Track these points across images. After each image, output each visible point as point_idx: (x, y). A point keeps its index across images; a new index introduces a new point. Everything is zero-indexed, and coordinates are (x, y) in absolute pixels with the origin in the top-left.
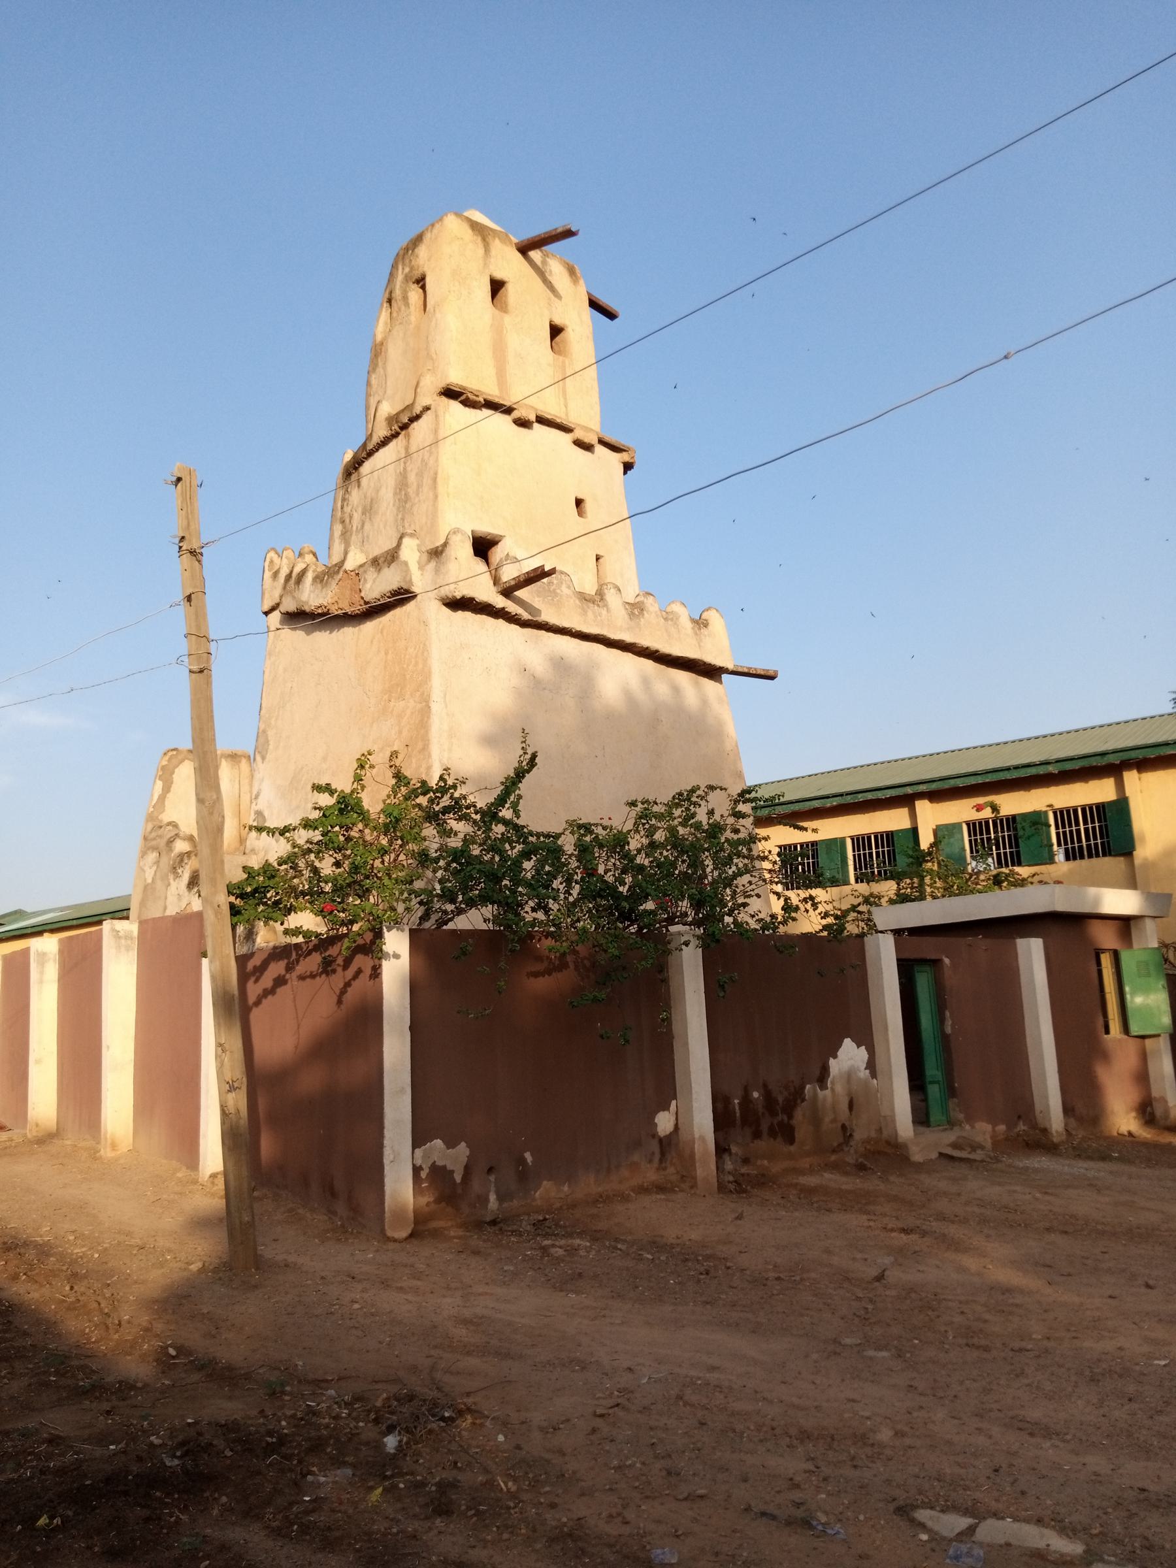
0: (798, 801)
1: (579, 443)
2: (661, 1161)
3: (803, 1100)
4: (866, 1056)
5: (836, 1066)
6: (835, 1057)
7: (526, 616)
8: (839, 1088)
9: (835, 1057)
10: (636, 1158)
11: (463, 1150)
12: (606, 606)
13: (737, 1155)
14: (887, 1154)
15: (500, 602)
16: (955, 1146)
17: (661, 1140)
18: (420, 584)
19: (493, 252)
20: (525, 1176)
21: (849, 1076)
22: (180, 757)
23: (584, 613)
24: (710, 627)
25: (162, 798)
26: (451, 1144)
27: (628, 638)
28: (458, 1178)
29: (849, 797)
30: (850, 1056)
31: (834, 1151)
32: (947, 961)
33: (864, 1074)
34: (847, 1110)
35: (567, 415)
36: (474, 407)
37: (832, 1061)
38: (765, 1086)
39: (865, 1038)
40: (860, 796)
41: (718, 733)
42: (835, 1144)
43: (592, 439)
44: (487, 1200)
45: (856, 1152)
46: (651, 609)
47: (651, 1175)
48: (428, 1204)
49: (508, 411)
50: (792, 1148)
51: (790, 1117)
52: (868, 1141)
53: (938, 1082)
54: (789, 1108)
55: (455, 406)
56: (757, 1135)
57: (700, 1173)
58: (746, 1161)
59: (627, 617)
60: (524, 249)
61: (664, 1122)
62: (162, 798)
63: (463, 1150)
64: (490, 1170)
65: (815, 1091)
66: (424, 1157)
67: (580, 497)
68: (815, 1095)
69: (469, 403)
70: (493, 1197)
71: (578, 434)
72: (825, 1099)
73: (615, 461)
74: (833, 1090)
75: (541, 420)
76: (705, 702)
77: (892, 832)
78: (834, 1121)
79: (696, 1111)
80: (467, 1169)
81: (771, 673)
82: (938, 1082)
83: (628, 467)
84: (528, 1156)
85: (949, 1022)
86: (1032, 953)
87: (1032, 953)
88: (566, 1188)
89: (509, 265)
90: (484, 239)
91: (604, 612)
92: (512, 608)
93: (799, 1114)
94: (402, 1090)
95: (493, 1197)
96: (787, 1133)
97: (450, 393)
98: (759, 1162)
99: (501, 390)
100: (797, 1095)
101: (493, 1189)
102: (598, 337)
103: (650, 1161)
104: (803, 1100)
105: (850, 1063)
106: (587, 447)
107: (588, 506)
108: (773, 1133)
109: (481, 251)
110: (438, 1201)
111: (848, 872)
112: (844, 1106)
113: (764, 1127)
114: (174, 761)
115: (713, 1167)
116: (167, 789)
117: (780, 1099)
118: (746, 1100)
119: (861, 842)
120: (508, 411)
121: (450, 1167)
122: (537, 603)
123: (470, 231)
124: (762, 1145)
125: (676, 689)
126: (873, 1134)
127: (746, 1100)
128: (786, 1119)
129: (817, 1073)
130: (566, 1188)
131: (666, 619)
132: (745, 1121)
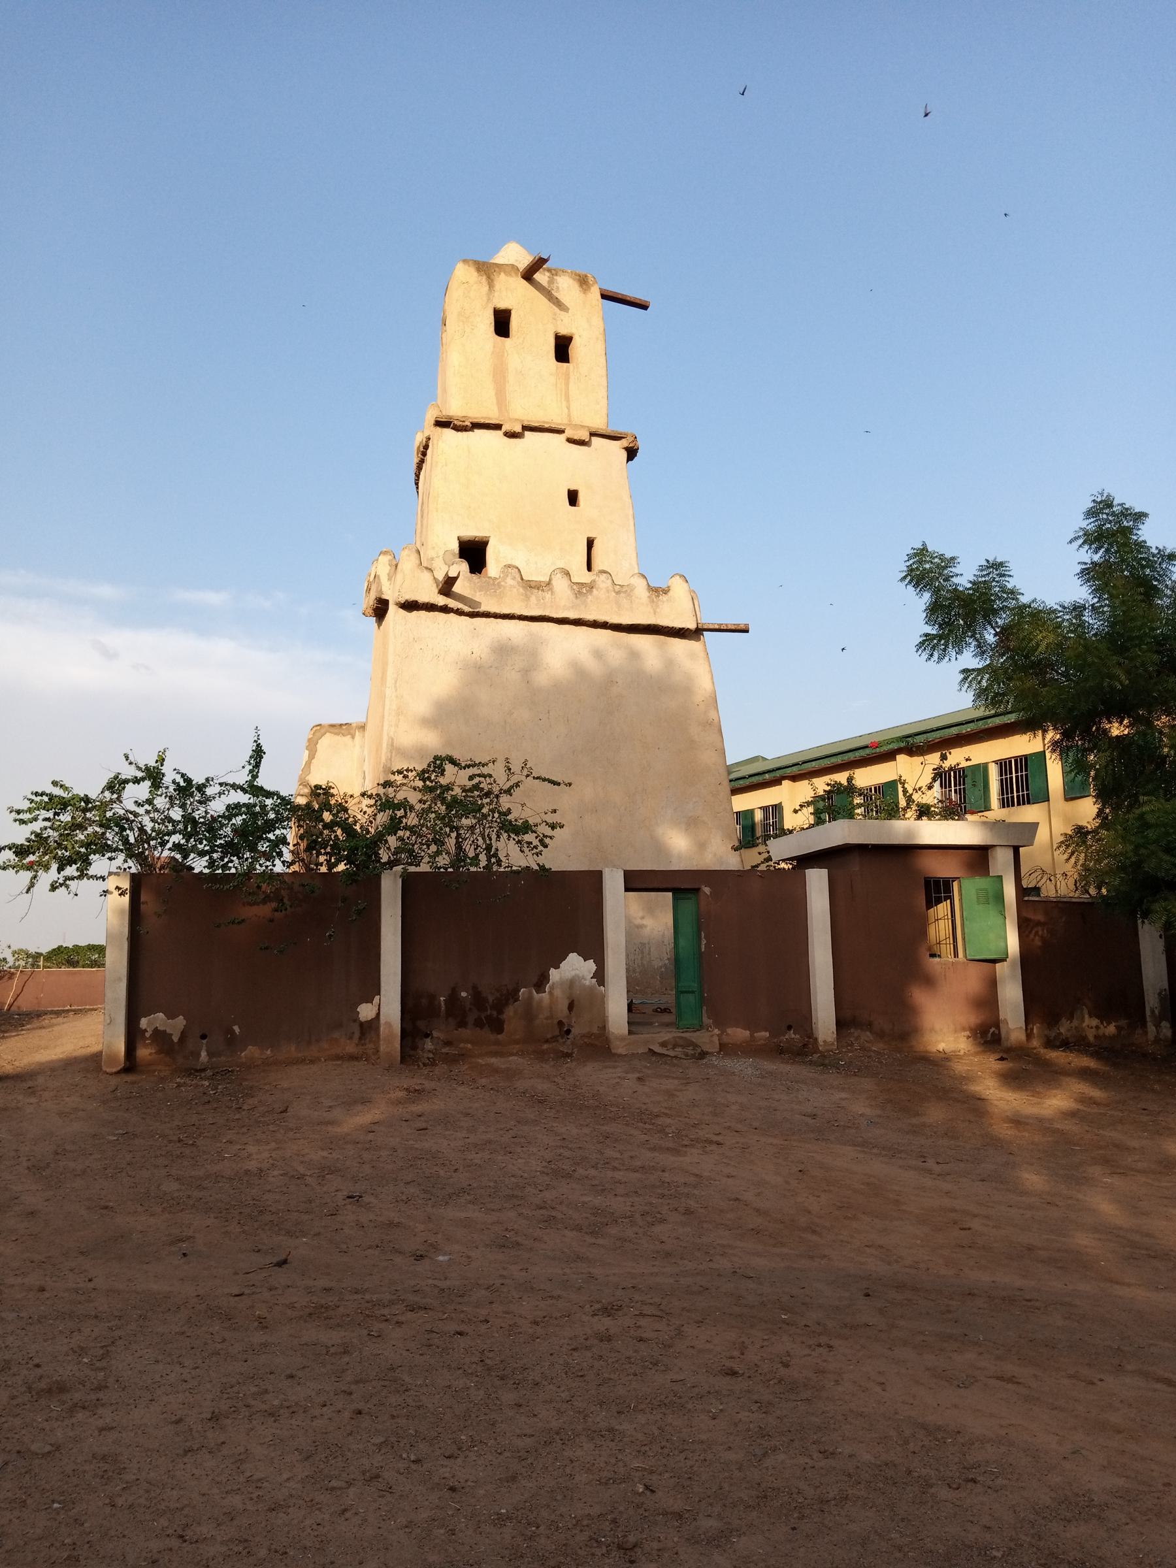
0: (938, 729)
1: (570, 441)
2: (360, 1039)
3: (517, 1000)
4: (594, 967)
5: (554, 975)
6: (557, 967)
7: (467, 609)
8: (558, 993)
9: (557, 967)
10: (336, 1035)
11: (180, 1021)
12: (551, 590)
13: (438, 1038)
14: (598, 1046)
15: (441, 601)
16: (663, 1044)
17: (362, 1024)
18: (389, 592)
19: (497, 286)
20: (231, 1042)
21: (572, 983)
22: (323, 731)
23: (527, 598)
24: (670, 593)
25: (308, 764)
26: (171, 1016)
27: (572, 615)
28: (175, 1039)
29: (981, 723)
30: (575, 967)
31: (547, 1041)
32: (707, 890)
33: (589, 981)
34: (566, 1010)
35: (569, 415)
36: (466, 430)
37: (552, 971)
38: (475, 988)
39: (594, 950)
40: (989, 721)
41: (687, 689)
42: (549, 1036)
43: (584, 436)
44: (199, 1055)
45: (573, 1044)
46: (602, 585)
47: (351, 1048)
48: (151, 1054)
49: (498, 427)
50: (500, 1037)
51: (501, 1012)
52: (590, 1035)
53: (693, 992)
54: (500, 1006)
55: (448, 433)
56: (462, 1024)
57: (383, 1048)
58: (448, 1043)
59: (572, 597)
60: (528, 275)
61: (366, 1012)
62: (308, 764)
63: (180, 1021)
64: (204, 1037)
65: (530, 993)
66: (149, 1023)
67: (572, 488)
68: (531, 997)
69: (458, 429)
70: (204, 1054)
71: (569, 433)
72: (541, 1001)
73: (616, 450)
74: (551, 993)
75: (526, 428)
76: (670, 663)
77: (1026, 757)
78: (551, 1017)
79: (388, 1005)
80: (183, 1035)
81: (742, 627)
82: (693, 992)
83: (631, 453)
84: (236, 1029)
85: (704, 942)
86: (817, 881)
87: (817, 881)
88: (269, 1052)
89: (513, 294)
90: (489, 277)
91: (548, 595)
92: (452, 603)
93: (510, 1011)
94: (120, 979)
95: (204, 1054)
96: (497, 1026)
97: (441, 424)
98: (462, 1045)
99: (500, 409)
100: (513, 995)
101: (204, 1048)
102: (609, 337)
103: (351, 1038)
104: (517, 1000)
105: (573, 973)
106: (581, 443)
107: (581, 498)
108: (479, 1024)
109: (487, 288)
110: (159, 1052)
111: (989, 797)
112: (563, 1006)
113: (471, 1019)
114: (318, 734)
115: (398, 1046)
116: (312, 756)
117: (491, 999)
118: (453, 998)
119: (1004, 765)
120: (498, 427)
121: (168, 1031)
122: (478, 597)
123: (475, 274)
124: (466, 1033)
125: (634, 655)
126: (595, 1031)
127: (453, 998)
128: (495, 1013)
129: (535, 980)
130: (269, 1052)
131: (618, 593)
132: (449, 1013)
